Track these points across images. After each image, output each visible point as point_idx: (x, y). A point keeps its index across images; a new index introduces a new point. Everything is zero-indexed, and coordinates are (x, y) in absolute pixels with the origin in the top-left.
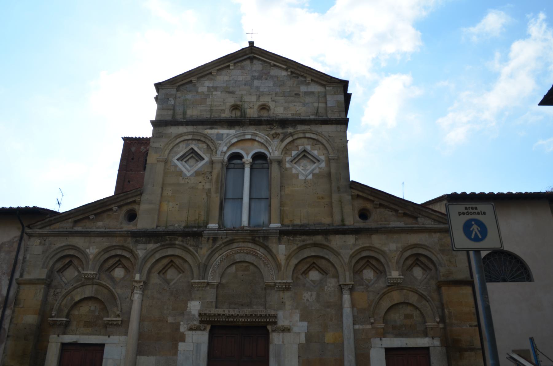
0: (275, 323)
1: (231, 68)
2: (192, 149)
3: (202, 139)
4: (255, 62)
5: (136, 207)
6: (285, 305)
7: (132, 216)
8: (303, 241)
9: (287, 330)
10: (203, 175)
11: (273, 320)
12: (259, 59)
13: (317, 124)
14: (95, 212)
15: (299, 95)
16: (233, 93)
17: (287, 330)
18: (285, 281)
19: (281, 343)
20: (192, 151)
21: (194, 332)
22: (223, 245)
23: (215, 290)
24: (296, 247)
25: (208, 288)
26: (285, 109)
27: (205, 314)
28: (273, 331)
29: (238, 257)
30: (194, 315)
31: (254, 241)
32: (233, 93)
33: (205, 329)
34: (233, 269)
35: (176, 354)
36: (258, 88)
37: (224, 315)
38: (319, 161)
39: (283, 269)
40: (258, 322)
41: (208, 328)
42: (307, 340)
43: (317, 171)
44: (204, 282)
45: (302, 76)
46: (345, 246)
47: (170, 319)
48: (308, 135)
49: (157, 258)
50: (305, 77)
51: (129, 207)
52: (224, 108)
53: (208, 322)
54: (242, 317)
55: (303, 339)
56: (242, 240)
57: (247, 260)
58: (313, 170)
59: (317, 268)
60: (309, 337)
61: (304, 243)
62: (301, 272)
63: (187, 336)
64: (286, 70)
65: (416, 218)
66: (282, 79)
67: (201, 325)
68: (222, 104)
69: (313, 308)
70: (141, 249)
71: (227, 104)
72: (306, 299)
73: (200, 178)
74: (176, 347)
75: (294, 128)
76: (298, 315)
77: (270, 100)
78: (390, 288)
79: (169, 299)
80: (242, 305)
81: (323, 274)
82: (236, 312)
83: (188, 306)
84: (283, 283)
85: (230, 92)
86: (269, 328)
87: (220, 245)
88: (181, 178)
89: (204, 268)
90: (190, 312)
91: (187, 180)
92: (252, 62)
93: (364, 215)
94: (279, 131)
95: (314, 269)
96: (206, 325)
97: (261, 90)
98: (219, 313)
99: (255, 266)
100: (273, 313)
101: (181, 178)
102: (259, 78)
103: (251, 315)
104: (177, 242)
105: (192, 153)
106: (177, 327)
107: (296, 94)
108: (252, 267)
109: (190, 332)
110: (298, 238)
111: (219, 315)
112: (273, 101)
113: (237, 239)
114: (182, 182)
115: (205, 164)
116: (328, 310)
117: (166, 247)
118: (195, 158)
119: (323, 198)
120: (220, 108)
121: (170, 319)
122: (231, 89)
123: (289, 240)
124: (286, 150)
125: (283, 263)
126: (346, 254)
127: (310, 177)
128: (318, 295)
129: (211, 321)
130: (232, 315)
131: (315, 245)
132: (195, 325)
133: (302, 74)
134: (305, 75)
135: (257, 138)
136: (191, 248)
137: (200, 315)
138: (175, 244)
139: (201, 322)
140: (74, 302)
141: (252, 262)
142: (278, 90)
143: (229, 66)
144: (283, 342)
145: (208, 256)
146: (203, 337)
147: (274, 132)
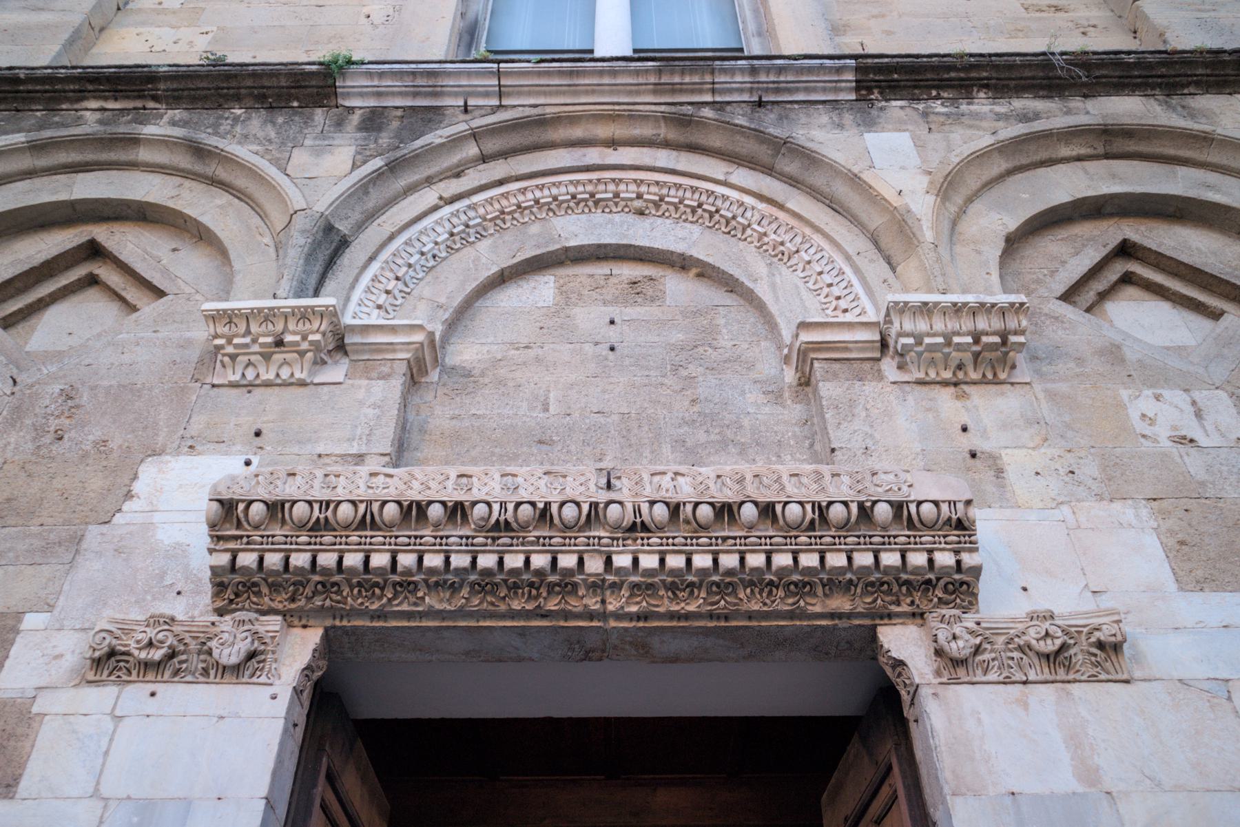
0: (960, 587)
6: (999, 472)
8: (1025, 118)
9: (1083, 654)
11: (945, 559)
17: (1083, 654)
18: (970, 298)
21: (135, 695)
22: (472, 150)
23: (396, 385)
24: (986, 141)
25: (336, 372)
28: (954, 665)
29: (576, 230)
30: (179, 552)
31: (684, 132)
33: (252, 662)
34: (542, 291)
37: (457, 511)
39: (928, 235)
40: (801, 584)
41: (298, 650)
44: (304, 315)
53: (290, 592)
54: (638, 528)
56: (603, 131)
61: (1038, 126)
62: (1061, 289)
63: (47, 734)
67: (226, 623)
72: (1163, 432)
81: (1216, 315)
82: (573, 490)
83: (137, 487)
84: (957, 309)
86: (902, 642)
87: (455, 142)
89: (330, 247)
90: (148, 526)
95: (1131, 291)
96: (273, 623)
99: (706, 272)
100: (930, 488)
103: (726, 512)
104: (150, 130)
108: (676, 286)
109: (102, 697)
110: (982, 105)
111: (414, 512)
113: (573, 120)
117: (62, 157)
123: (925, 115)
125: (921, 204)
130: (544, 515)
131: (1113, 142)
136: (242, 152)
138: (134, 141)
139: (233, 588)
141: (679, 248)
145: (364, 187)
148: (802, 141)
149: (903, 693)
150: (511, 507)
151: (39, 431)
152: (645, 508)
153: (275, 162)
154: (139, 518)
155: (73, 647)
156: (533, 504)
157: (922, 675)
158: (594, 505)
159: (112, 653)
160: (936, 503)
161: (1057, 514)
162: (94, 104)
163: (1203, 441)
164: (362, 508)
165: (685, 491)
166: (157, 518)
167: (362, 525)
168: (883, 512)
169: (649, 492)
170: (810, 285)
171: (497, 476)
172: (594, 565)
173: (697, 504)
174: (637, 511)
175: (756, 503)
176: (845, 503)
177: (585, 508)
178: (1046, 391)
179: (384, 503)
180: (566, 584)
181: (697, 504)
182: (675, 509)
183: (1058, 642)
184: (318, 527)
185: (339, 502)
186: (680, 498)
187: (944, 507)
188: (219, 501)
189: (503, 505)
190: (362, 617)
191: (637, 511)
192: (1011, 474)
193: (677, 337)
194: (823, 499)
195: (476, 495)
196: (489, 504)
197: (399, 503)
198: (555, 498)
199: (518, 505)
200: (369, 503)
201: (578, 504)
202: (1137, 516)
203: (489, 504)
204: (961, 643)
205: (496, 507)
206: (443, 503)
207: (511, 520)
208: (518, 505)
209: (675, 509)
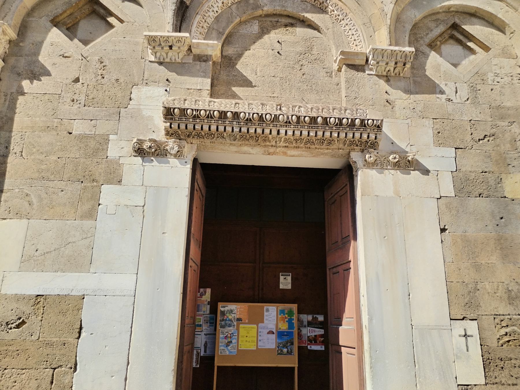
27: (183, 111)
41: (190, 151)
60: (464, 187)
76: (431, 131)
90: (139, 109)
98: (222, 109)
103: (314, 120)
111: (223, 115)
116: (504, 124)
128: (474, 89)
130: (261, 118)
137: (169, 113)
149: (354, 168)
150: (251, 115)
152: (290, 117)
154: (136, 107)
155: (129, 148)
156: (258, 114)
157: (360, 166)
158: (275, 115)
159: (139, 149)
160: (373, 120)
161: (407, 121)
163: (454, 101)
164: (208, 113)
165: (303, 112)
166: (142, 107)
167: (208, 117)
168: (357, 122)
169: (291, 113)
170: (346, 33)
171: (247, 104)
172: (274, 132)
173: (305, 117)
174: (288, 118)
175: (322, 117)
176: (348, 119)
177: (273, 116)
178: (413, 80)
179: (214, 111)
181: (305, 117)
182: (298, 118)
183: (397, 160)
184: (195, 117)
185: (201, 110)
186: (300, 114)
187: (375, 121)
188: (165, 107)
189: (249, 113)
191: (288, 118)
192: (396, 108)
194: (341, 117)
195: (241, 110)
196: (245, 113)
197: (218, 111)
198: (264, 112)
199: (253, 114)
200: (210, 111)
201: (271, 115)
202: (429, 123)
203: (245, 113)
204: (372, 158)
205: (247, 114)
206: (232, 112)
207: (251, 118)
208: (253, 114)
209: (298, 118)
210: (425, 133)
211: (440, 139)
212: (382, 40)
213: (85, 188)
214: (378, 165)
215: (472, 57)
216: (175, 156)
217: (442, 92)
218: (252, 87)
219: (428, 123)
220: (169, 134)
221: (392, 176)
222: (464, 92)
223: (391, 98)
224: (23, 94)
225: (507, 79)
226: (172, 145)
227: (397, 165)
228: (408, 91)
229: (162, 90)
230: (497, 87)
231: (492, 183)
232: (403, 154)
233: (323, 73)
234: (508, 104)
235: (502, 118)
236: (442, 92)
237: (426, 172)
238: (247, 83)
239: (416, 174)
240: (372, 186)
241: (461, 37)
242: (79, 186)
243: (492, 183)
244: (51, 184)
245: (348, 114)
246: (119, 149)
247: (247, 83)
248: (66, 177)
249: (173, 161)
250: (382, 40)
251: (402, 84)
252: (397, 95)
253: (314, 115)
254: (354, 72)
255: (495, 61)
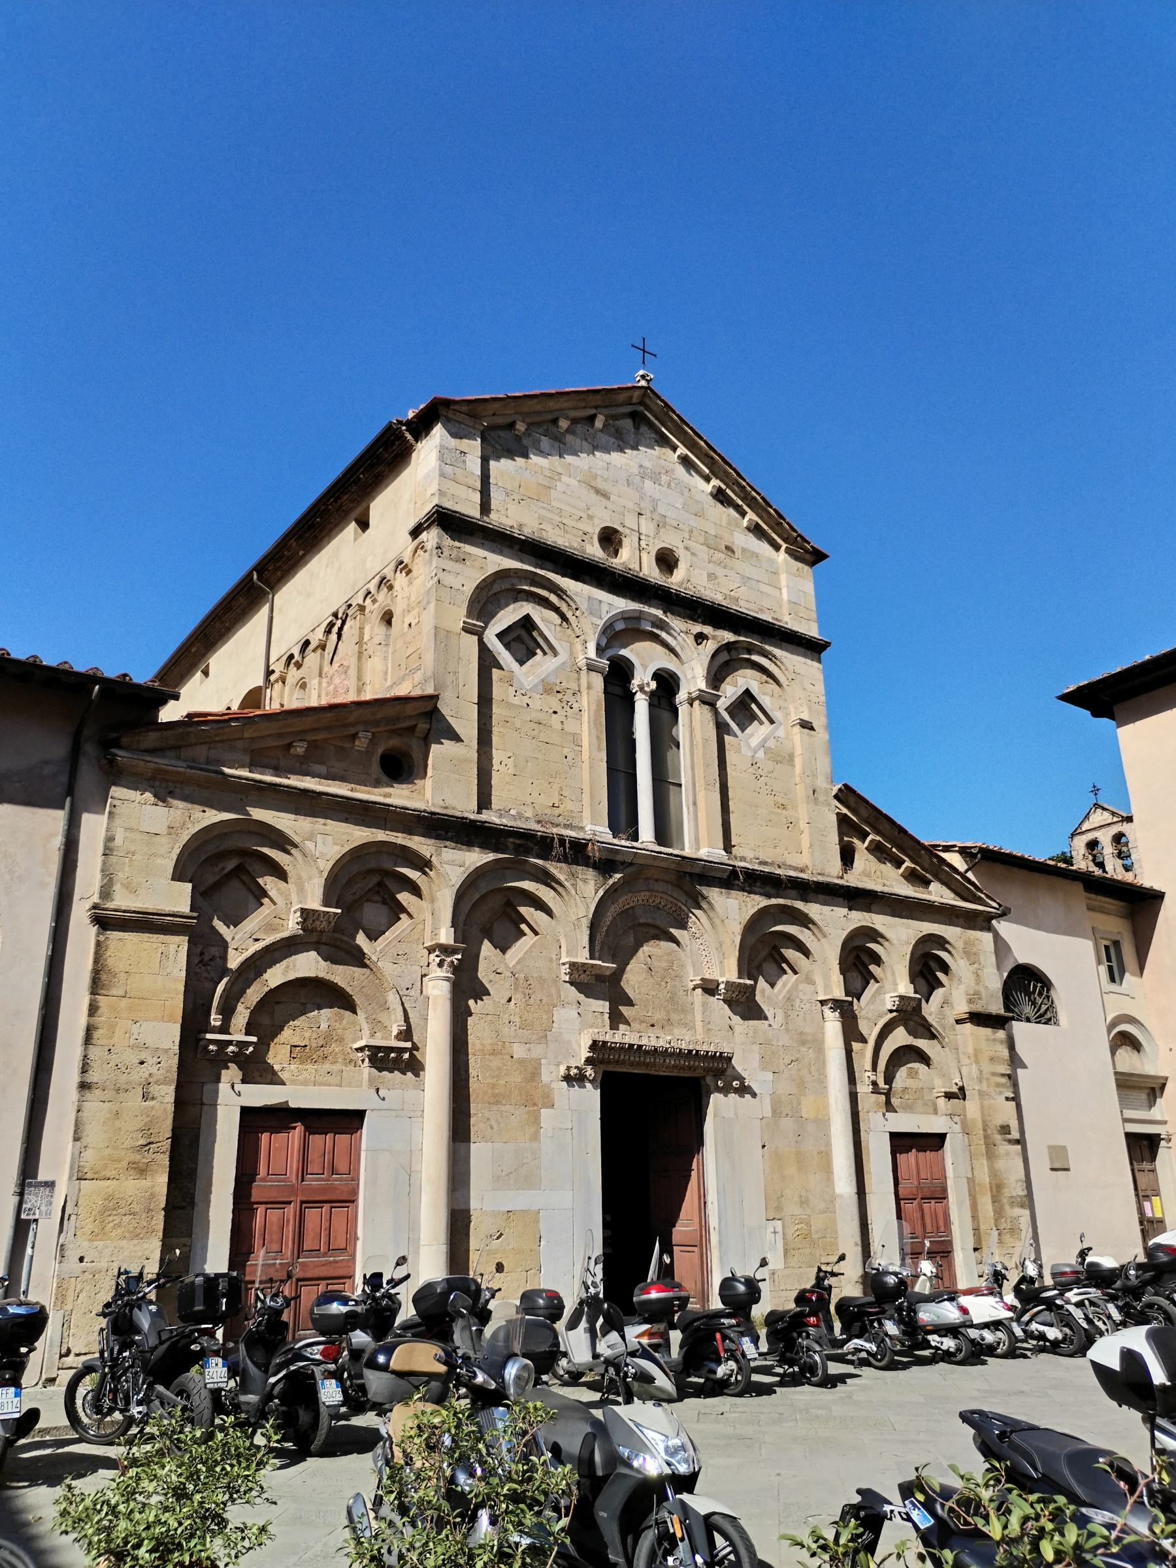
1: (599, 423)
2: (527, 619)
3: (553, 598)
4: (644, 429)
5: (415, 745)
7: (401, 767)
8: (769, 896)
10: (560, 696)
12: (651, 426)
13: (773, 637)
14: (310, 737)
15: (733, 552)
16: (605, 495)
19: (732, 1115)
20: (527, 623)
26: (712, 576)
28: (719, 1090)
32: (605, 495)
35: (536, 1137)
36: (655, 503)
37: (640, 1047)
38: (772, 722)
42: (774, 1111)
43: (771, 744)
45: (737, 508)
46: (835, 923)
47: (519, 1051)
48: (755, 658)
49: (484, 891)
50: (743, 514)
51: (394, 742)
52: (589, 529)
54: (672, 1055)
55: (768, 1111)
57: (659, 923)
58: (765, 740)
59: (777, 957)
63: (556, 1092)
64: (707, 479)
65: (926, 883)
66: (697, 497)
68: (584, 516)
69: (781, 1044)
70: (451, 863)
71: (596, 521)
73: (553, 702)
74: (536, 1121)
75: (736, 632)
76: (757, 1057)
77: (681, 545)
78: (895, 1014)
79: (510, 1000)
80: (653, 1026)
85: (598, 492)
88: (512, 690)
91: (526, 700)
92: (637, 427)
93: (847, 856)
94: (707, 630)
97: (661, 510)
101: (512, 690)
102: (656, 481)
103: (690, 1051)
105: (524, 626)
106: (533, 1072)
107: (727, 548)
111: (631, 1046)
112: (687, 548)
114: (516, 701)
115: (562, 667)
116: (804, 1049)
118: (523, 642)
119: (783, 806)
120: (580, 525)
121: (519, 1051)
122: (601, 485)
124: (717, 676)
126: (838, 937)
127: (760, 754)
128: (787, 1016)
129: (609, 1062)
132: (577, 1067)
133: (740, 502)
134: (745, 507)
135: (664, 635)
140: (266, 989)
142: (692, 523)
143: (592, 419)
144: (736, 1114)
146: (591, 1097)
147: (698, 628)
148: (711, 899)
151: (524, 994)
153: (573, 885)
162: (511, 840)
165: (683, 1047)
180: (654, 1064)
190: (611, 1068)
193: (664, 964)
210: (755, 1061)
211: (766, 1063)
212: (733, 977)
213: (529, 1112)
214: (726, 1090)
215: (785, 977)
216: (590, 1081)
217: (766, 1018)
218: (633, 1005)
219: (756, 1047)
220: (588, 1061)
221: (733, 1096)
222: (780, 1018)
223: (732, 1023)
224: (471, 1014)
225: (808, 1005)
226: (589, 1072)
227: (736, 1091)
228: (744, 1018)
229: (574, 1013)
230: (801, 1014)
231: (795, 1105)
232: (741, 1079)
233: (682, 993)
234: (807, 1030)
235: (803, 1043)
236: (766, 1018)
237: (754, 1095)
238: (630, 1003)
239: (748, 1096)
240: (720, 1109)
241: (777, 957)
242: (523, 1110)
243: (795, 1105)
244: (503, 1108)
245: (712, 1049)
246: (552, 1074)
247: (630, 1003)
248: (513, 1101)
249: (588, 1085)
250: (733, 977)
251: (739, 1009)
252: (737, 1019)
253: (691, 1048)
254: (707, 996)
255: (801, 987)
